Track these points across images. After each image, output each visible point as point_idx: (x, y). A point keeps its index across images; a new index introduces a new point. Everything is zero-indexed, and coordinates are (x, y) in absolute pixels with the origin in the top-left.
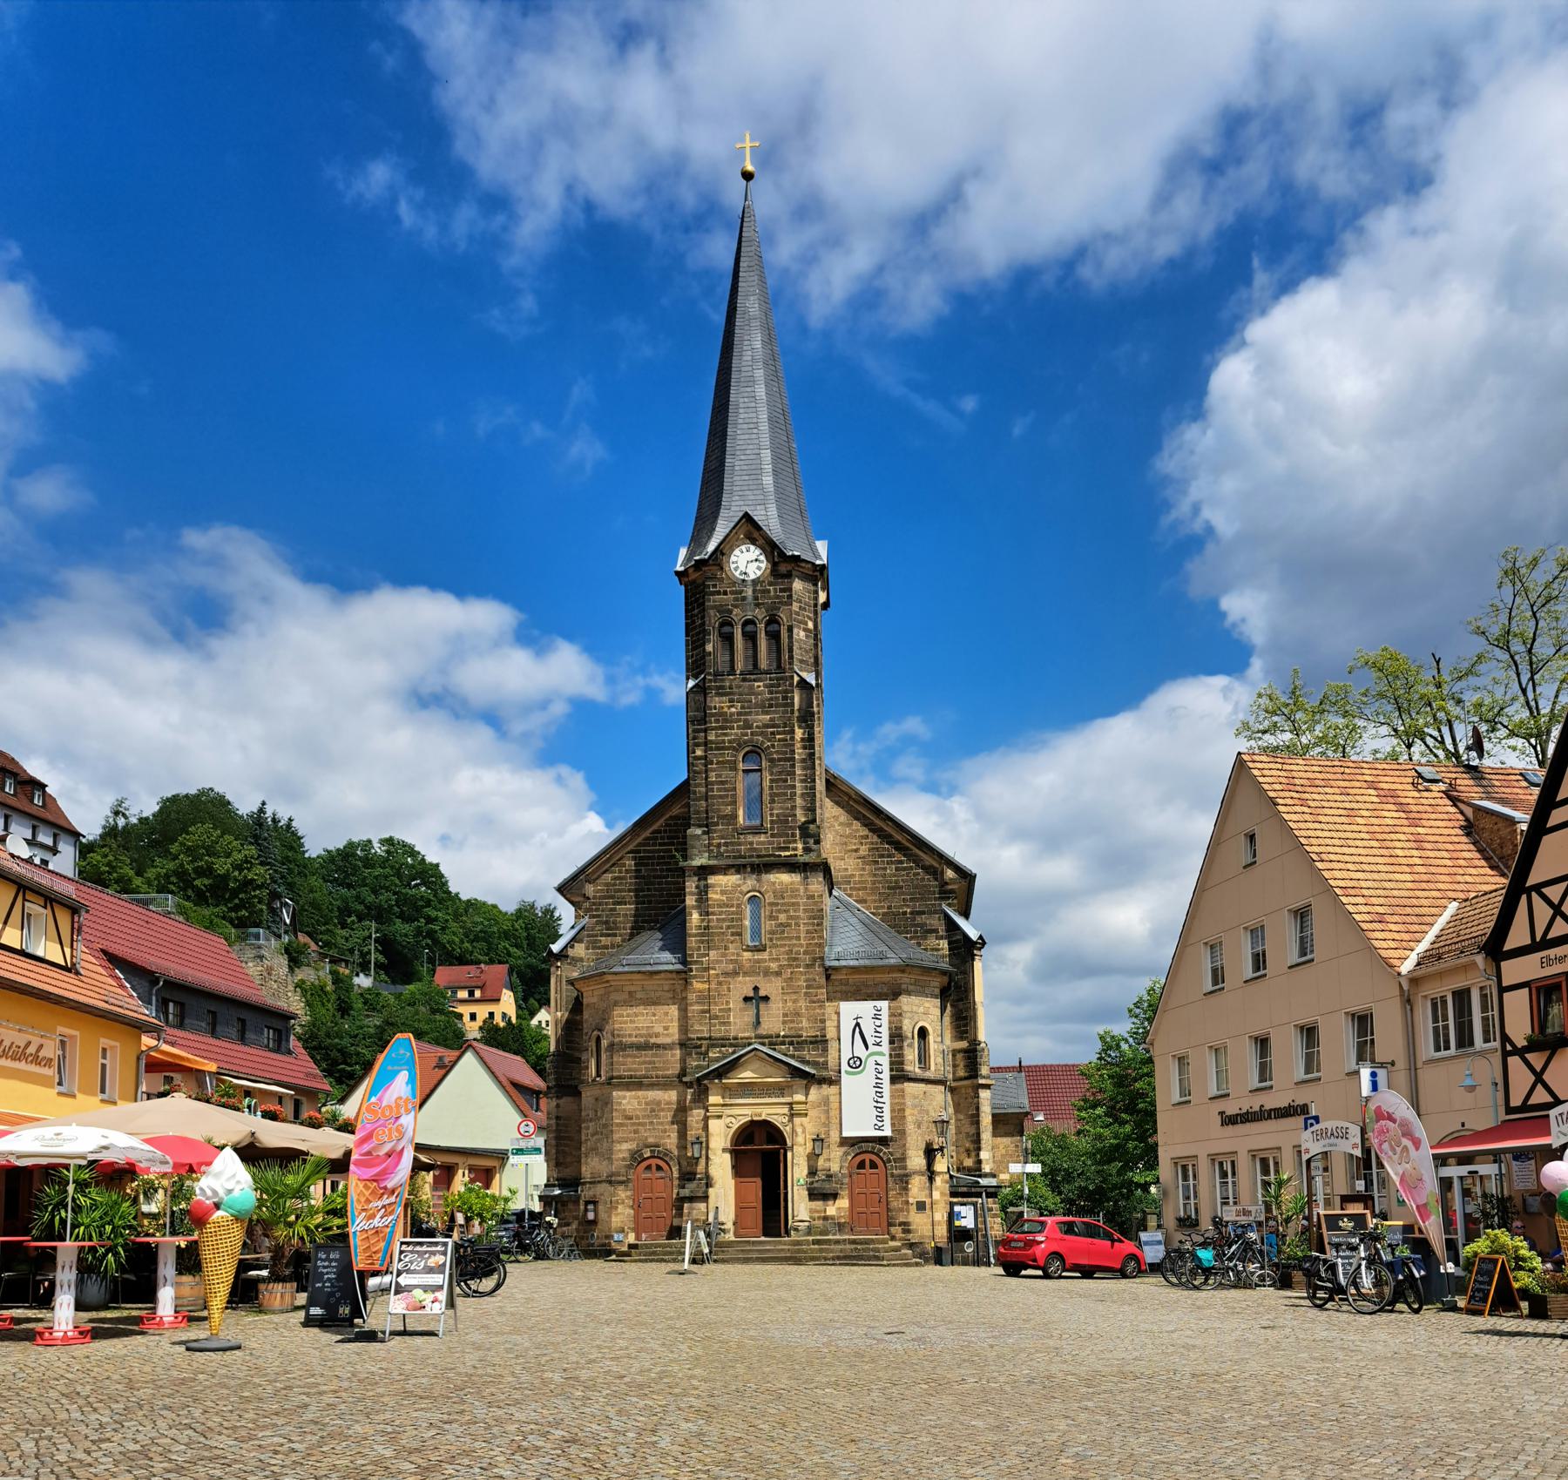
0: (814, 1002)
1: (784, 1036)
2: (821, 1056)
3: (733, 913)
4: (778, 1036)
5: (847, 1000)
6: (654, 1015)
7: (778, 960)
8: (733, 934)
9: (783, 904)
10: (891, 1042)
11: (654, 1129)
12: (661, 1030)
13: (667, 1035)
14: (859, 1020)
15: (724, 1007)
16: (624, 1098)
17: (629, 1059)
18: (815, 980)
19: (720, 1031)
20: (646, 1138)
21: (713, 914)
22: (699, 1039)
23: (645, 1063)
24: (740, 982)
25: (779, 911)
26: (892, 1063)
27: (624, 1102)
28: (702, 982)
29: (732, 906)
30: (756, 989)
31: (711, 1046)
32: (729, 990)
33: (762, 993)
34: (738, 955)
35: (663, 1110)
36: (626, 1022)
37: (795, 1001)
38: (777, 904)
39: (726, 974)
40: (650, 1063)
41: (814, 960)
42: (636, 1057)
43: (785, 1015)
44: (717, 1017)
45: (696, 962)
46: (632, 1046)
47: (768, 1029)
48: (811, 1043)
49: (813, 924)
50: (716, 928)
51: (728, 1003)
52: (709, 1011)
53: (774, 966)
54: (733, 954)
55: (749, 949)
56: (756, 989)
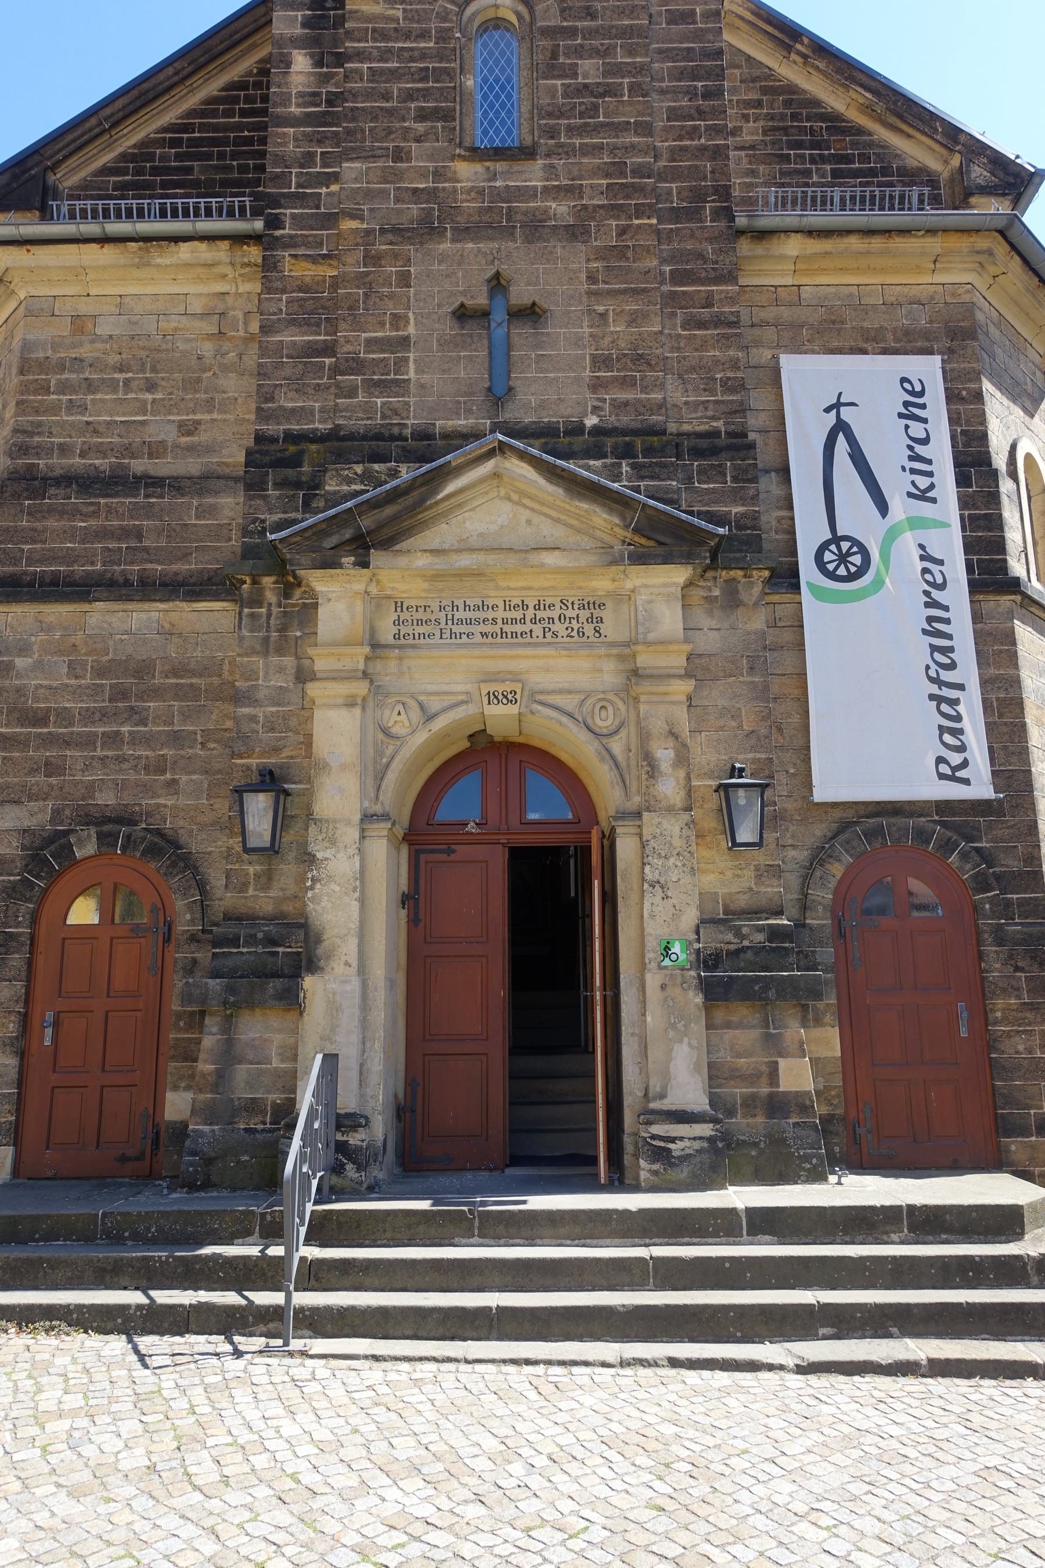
0: (702, 325)
1: (597, 431)
2: (737, 496)
3: (424, 55)
4: (578, 429)
5: (798, 349)
6: (151, 386)
7: (572, 191)
8: (422, 116)
9: (589, 34)
10: (962, 480)
11: (121, 759)
12: (169, 434)
13: (191, 449)
14: (846, 413)
15: (388, 333)
16: (24, 650)
17: (52, 523)
18: (701, 256)
19: (369, 409)
20: (91, 788)
21: (360, 55)
22: (291, 437)
23: (104, 534)
24: (443, 258)
25: (579, 52)
26: (969, 547)
27: (20, 662)
28: (314, 260)
29: (424, 35)
30: (497, 284)
31: (341, 457)
32: (404, 280)
33: (521, 294)
34: (439, 174)
35: (156, 693)
36: (54, 409)
37: (634, 319)
38: (572, 32)
39: (398, 232)
40: (125, 533)
41: (699, 196)
42: (75, 513)
43: (601, 362)
44: (356, 365)
45: (299, 199)
46: (67, 480)
47: (542, 405)
48: (698, 453)
49: (692, 94)
50: (369, 95)
51: (398, 321)
52: (328, 350)
53: (560, 209)
54: (423, 174)
55: (475, 154)
56: (497, 284)
